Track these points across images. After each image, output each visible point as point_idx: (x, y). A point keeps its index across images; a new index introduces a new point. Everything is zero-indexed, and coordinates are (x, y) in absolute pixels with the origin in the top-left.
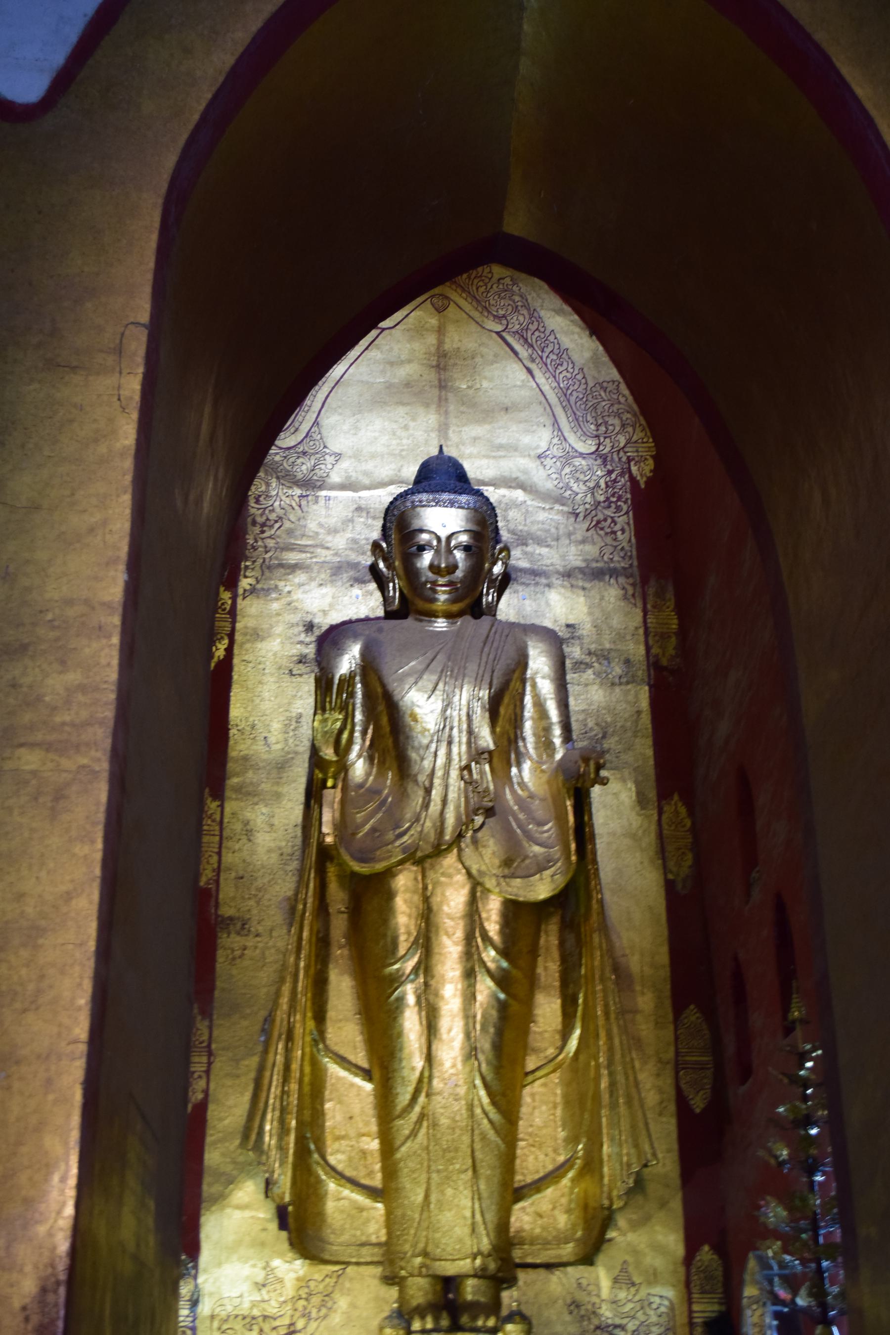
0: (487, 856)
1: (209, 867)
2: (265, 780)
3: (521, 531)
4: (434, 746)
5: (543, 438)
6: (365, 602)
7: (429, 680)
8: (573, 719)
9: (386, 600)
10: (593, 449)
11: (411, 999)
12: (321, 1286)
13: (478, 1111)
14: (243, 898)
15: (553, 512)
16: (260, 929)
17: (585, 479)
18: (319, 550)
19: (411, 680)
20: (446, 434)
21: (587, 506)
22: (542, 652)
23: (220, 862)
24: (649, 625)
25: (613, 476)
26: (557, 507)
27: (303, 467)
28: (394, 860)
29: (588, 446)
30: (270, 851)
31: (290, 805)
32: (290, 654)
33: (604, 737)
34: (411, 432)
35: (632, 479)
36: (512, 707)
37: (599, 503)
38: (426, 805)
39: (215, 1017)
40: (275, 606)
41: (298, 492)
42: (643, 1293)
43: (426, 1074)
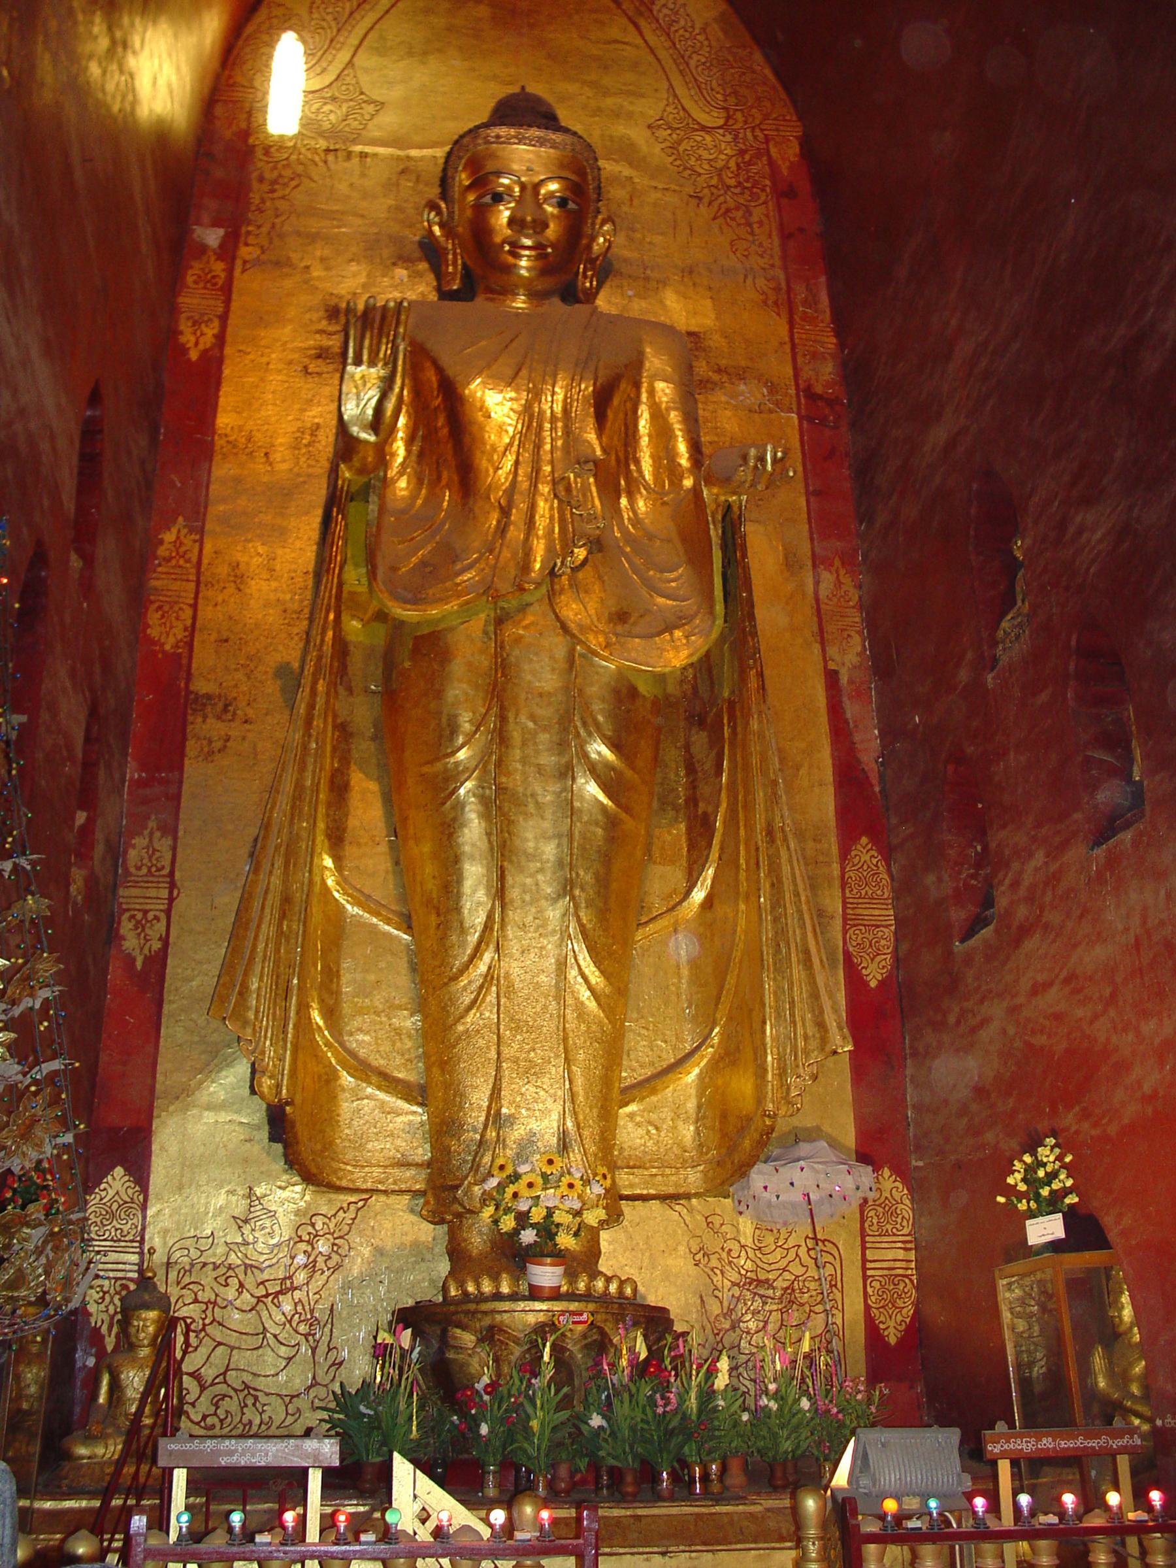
1: (180, 625)
2: (264, 509)
10: (721, 122)
12: (332, 1226)
13: (573, 973)
14: (227, 668)
16: (251, 713)
23: (194, 618)
24: (797, 341)
25: (747, 157)
30: (267, 604)
35: (771, 163)
36: (621, 415)
37: (729, 187)
38: (502, 530)
39: (181, 834)
40: (288, 284)
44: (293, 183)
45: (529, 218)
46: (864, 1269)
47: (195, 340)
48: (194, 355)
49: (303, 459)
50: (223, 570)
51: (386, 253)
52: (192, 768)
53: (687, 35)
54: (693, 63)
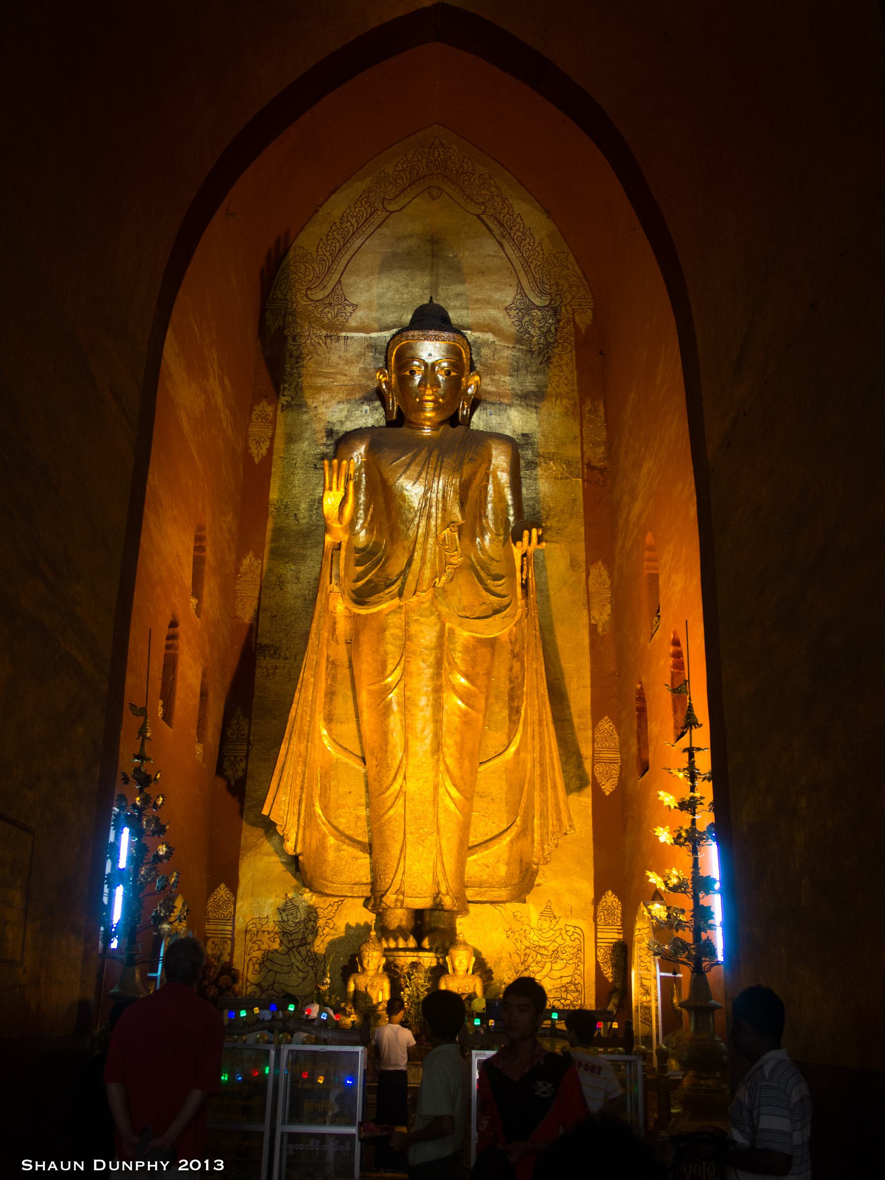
4: (417, 519)
6: (369, 417)
8: (525, 504)
9: (387, 413)
10: (547, 303)
15: (515, 350)
16: (288, 654)
20: (436, 290)
21: (541, 346)
25: (561, 324)
26: (518, 346)
27: (329, 315)
30: (296, 597)
31: (312, 564)
33: (547, 518)
34: (410, 289)
35: (576, 326)
40: (305, 417)
41: (324, 333)
42: (561, 924)
46: (596, 942)
47: (258, 452)
51: (358, 396)
53: (530, 248)
54: (532, 268)
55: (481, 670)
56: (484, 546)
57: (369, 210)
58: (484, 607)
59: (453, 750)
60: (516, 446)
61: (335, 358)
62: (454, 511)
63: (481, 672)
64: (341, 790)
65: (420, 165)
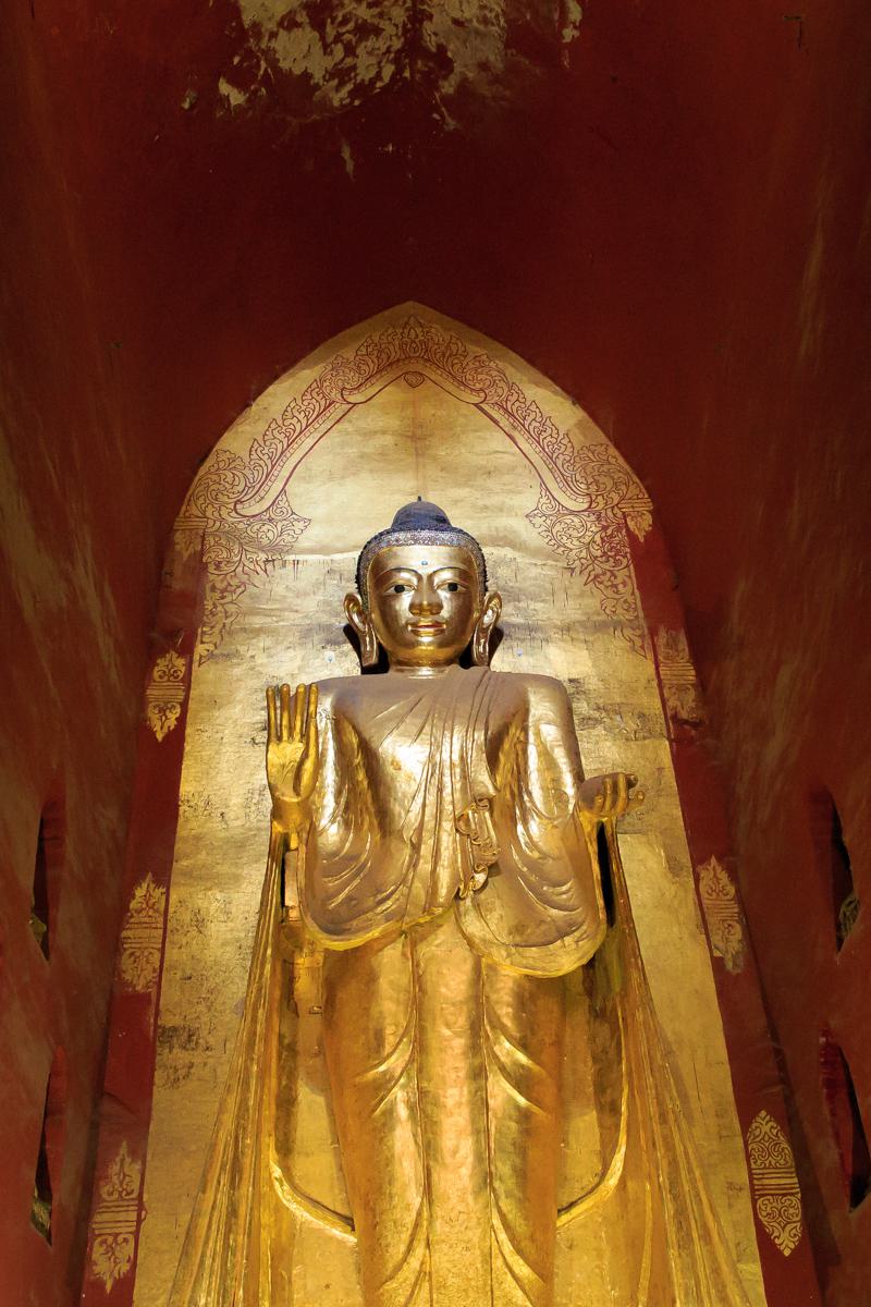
0: (489, 924)
1: (150, 968)
2: (220, 861)
3: (512, 587)
5: (529, 499)
7: (415, 725)
10: (586, 506)
11: (402, 1112)
14: (189, 1002)
16: (212, 1041)
17: (580, 533)
18: (287, 613)
19: (392, 724)
21: (583, 561)
22: (544, 697)
24: (662, 677)
26: (550, 562)
27: (269, 533)
28: (375, 933)
29: (581, 504)
30: (224, 944)
32: (254, 721)
36: (513, 756)
38: (414, 865)
39: (149, 1158)
40: (237, 671)
41: (263, 556)
43: (425, 1214)
44: (240, 590)
45: (425, 603)
48: (160, 736)
49: (253, 816)
50: (187, 917)
52: (160, 1095)
54: (559, 463)
55: (546, 1035)
56: (530, 837)
57: (323, 402)
58: (543, 927)
59: (511, 1183)
60: (565, 695)
61: (280, 590)
62: (480, 778)
63: (547, 1040)
64: (311, 1284)
65: (392, 348)
